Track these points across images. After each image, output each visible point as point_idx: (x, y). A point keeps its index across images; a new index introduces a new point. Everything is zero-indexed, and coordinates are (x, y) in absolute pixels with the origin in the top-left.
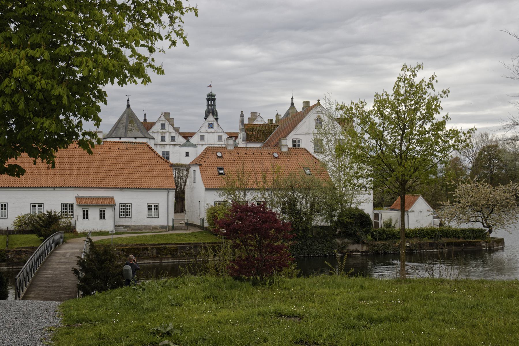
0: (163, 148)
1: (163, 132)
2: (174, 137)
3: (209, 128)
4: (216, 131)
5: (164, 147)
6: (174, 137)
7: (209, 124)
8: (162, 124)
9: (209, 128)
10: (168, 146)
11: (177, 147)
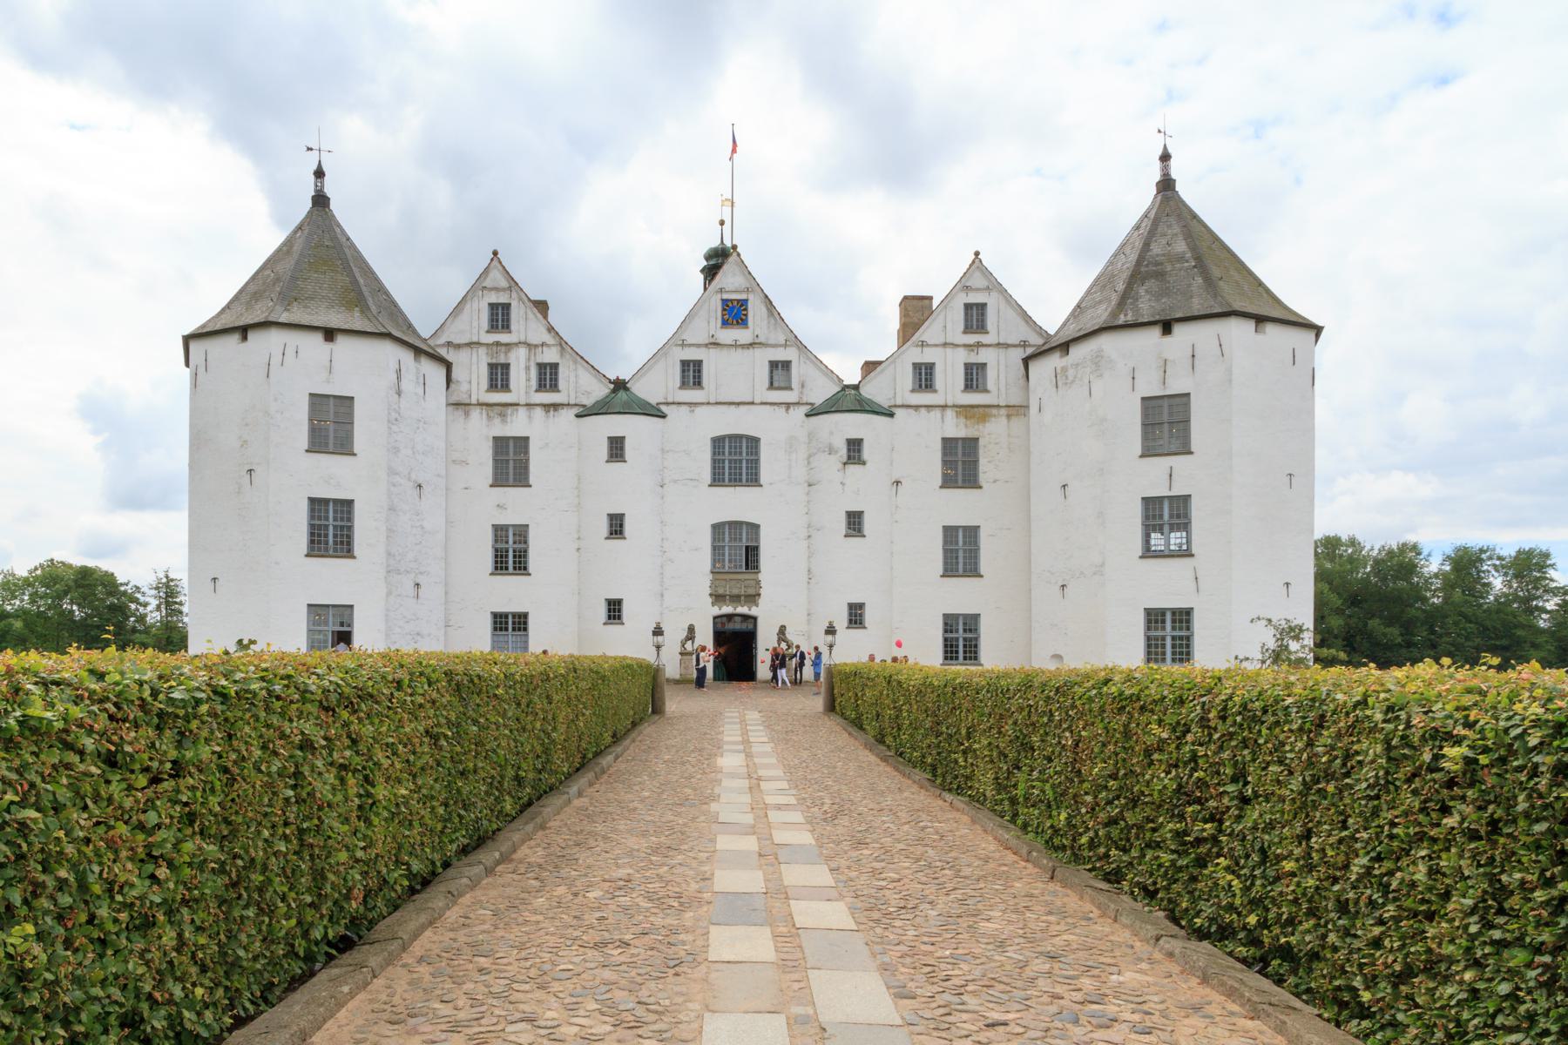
0: (497, 421)
1: (498, 344)
2: (555, 366)
3: (725, 323)
4: (762, 339)
5: (503, 416)
6: (555, 366)
8: (493, 306)
9: (725, 323)
10: (522, 411)
11: (568, 415)
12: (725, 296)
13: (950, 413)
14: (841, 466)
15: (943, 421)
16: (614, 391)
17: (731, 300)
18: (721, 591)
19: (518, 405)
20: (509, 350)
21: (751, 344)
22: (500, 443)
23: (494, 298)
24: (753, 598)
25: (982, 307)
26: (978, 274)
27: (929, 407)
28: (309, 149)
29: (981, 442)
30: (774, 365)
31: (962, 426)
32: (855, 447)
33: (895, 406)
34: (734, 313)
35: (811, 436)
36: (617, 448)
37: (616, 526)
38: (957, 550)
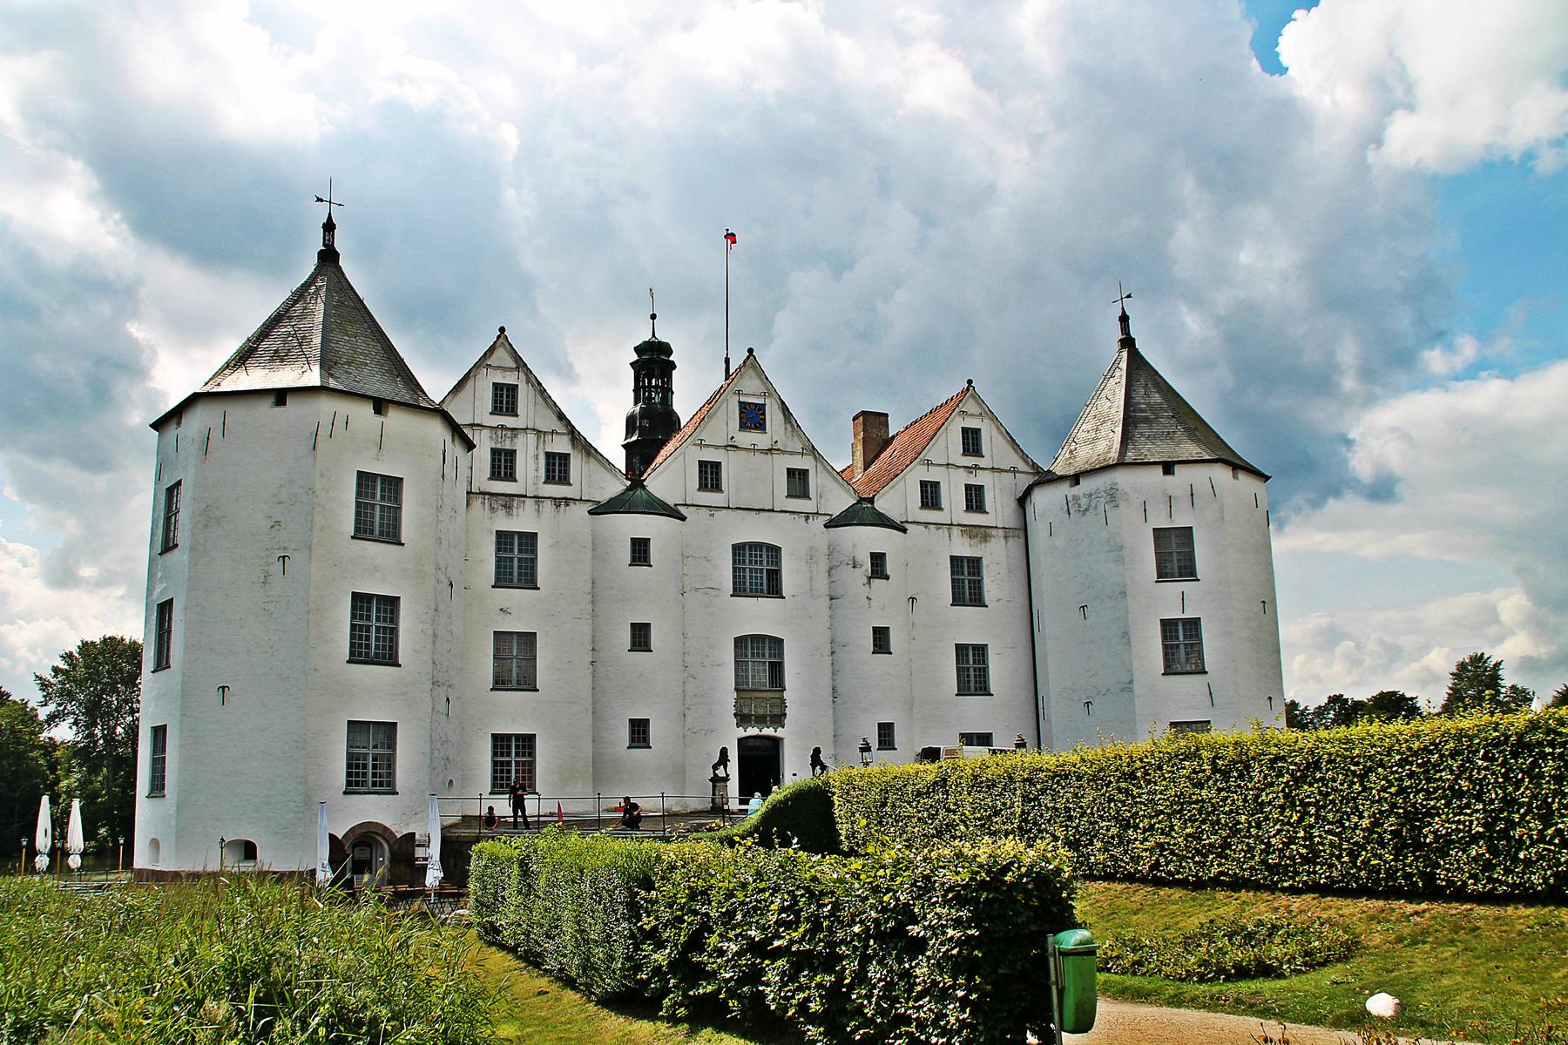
0: (501, 513)
1: (503, 427)
3: (743, 426)
4: (778, 446)
5: (508, 508)
7: (743, 406)
9: (743, 426)
13: (956, 531)
14: (866, 580)
16: (629, 489)
18: (746, 711)
19: (525, 496)
20: (516, 436)
21: (770, 450)
22: (503, 539)
23: (500, 378)
24: (778, 719)
26: (971, 401)
28: (320, 200)
31: (967, 544)
32: (878, 560)
33: (907, 522)
34: (752, 417)
35: (832, 550)
36: (640, 551)
37: (641, 637)
38: (968, 668)
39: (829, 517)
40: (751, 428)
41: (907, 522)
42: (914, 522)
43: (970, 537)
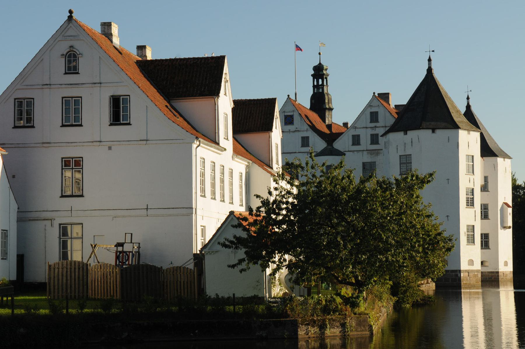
12: (286, 114)
15: (363, 156)
17: (288, 116)
21: (295, 131)
25: (377, 113)
27: (358, 151)
29: (377, 163)
30: (303, 138)
33: (345, 151)
39: (316, 153)
40: (288, 124)
41: (345, 151)
42: (349, 151)
43: (371, 154)
